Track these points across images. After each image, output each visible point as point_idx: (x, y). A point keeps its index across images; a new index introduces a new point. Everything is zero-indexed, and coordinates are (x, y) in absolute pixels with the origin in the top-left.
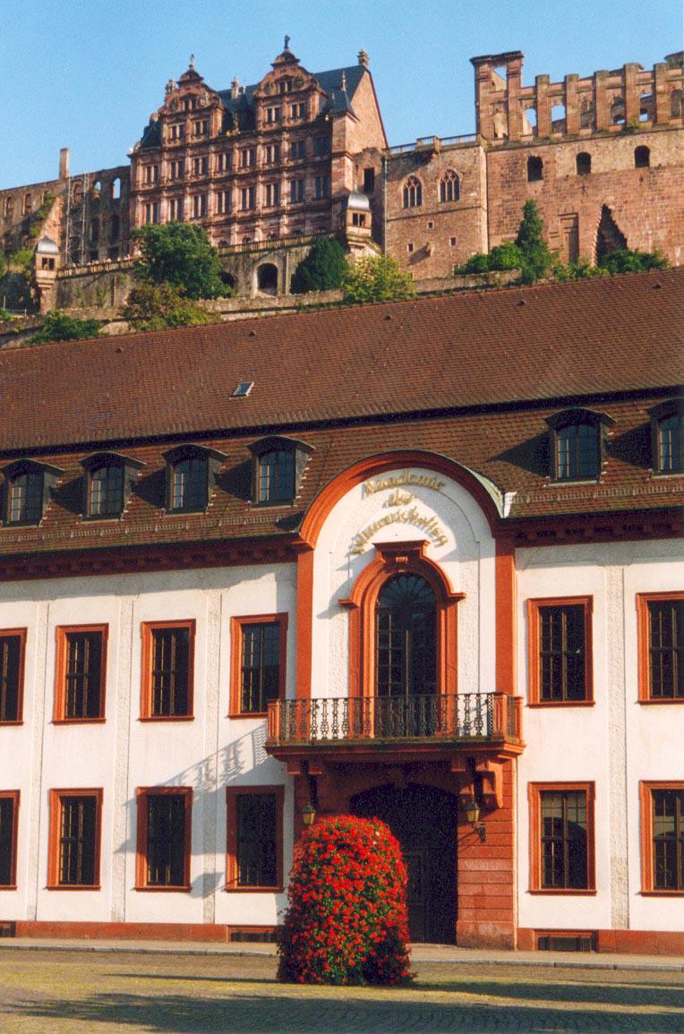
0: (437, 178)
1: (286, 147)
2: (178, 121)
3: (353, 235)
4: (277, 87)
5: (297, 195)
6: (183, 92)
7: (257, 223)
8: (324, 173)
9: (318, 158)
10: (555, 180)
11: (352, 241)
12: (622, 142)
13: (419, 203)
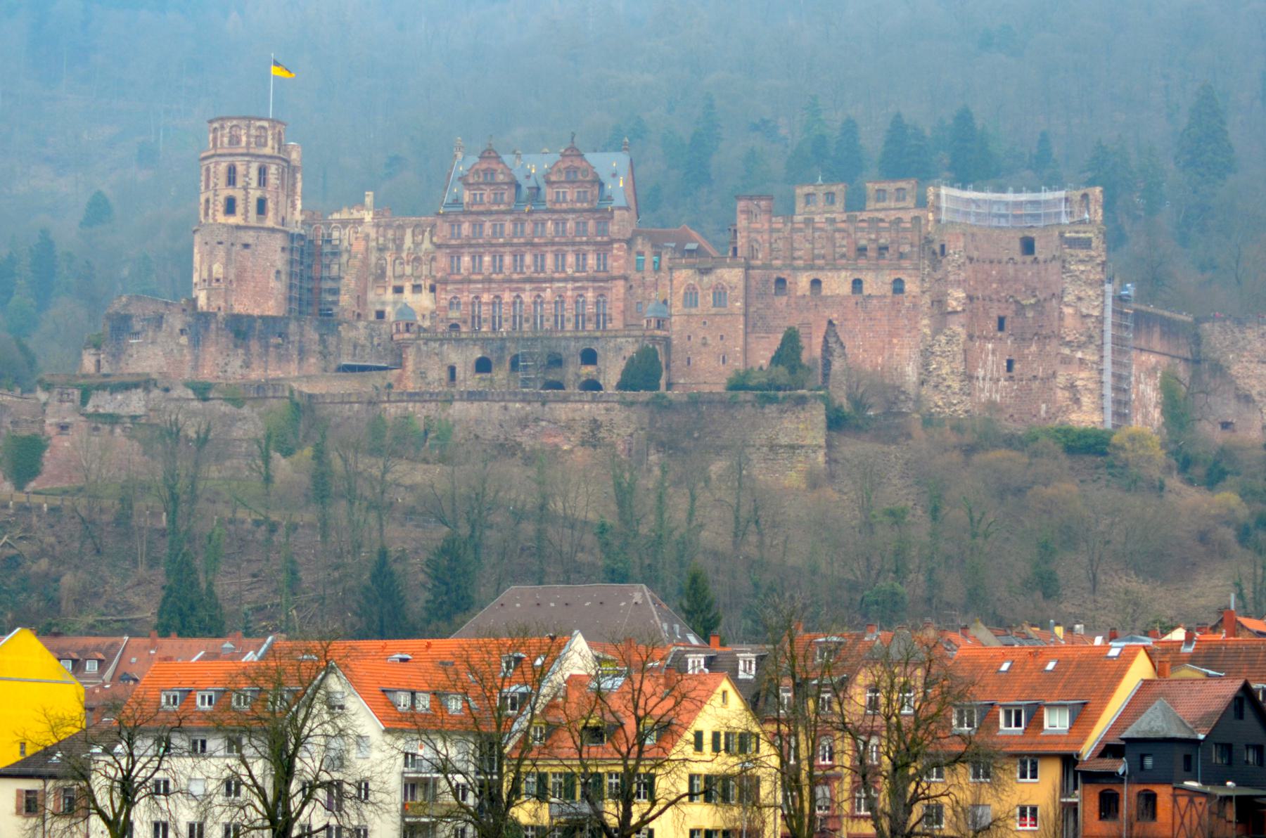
5: (581, 266)
6: (484, 166)
8: (603, 248)
9: (599, 239)
12: (843, 274)
13: (696, 305)
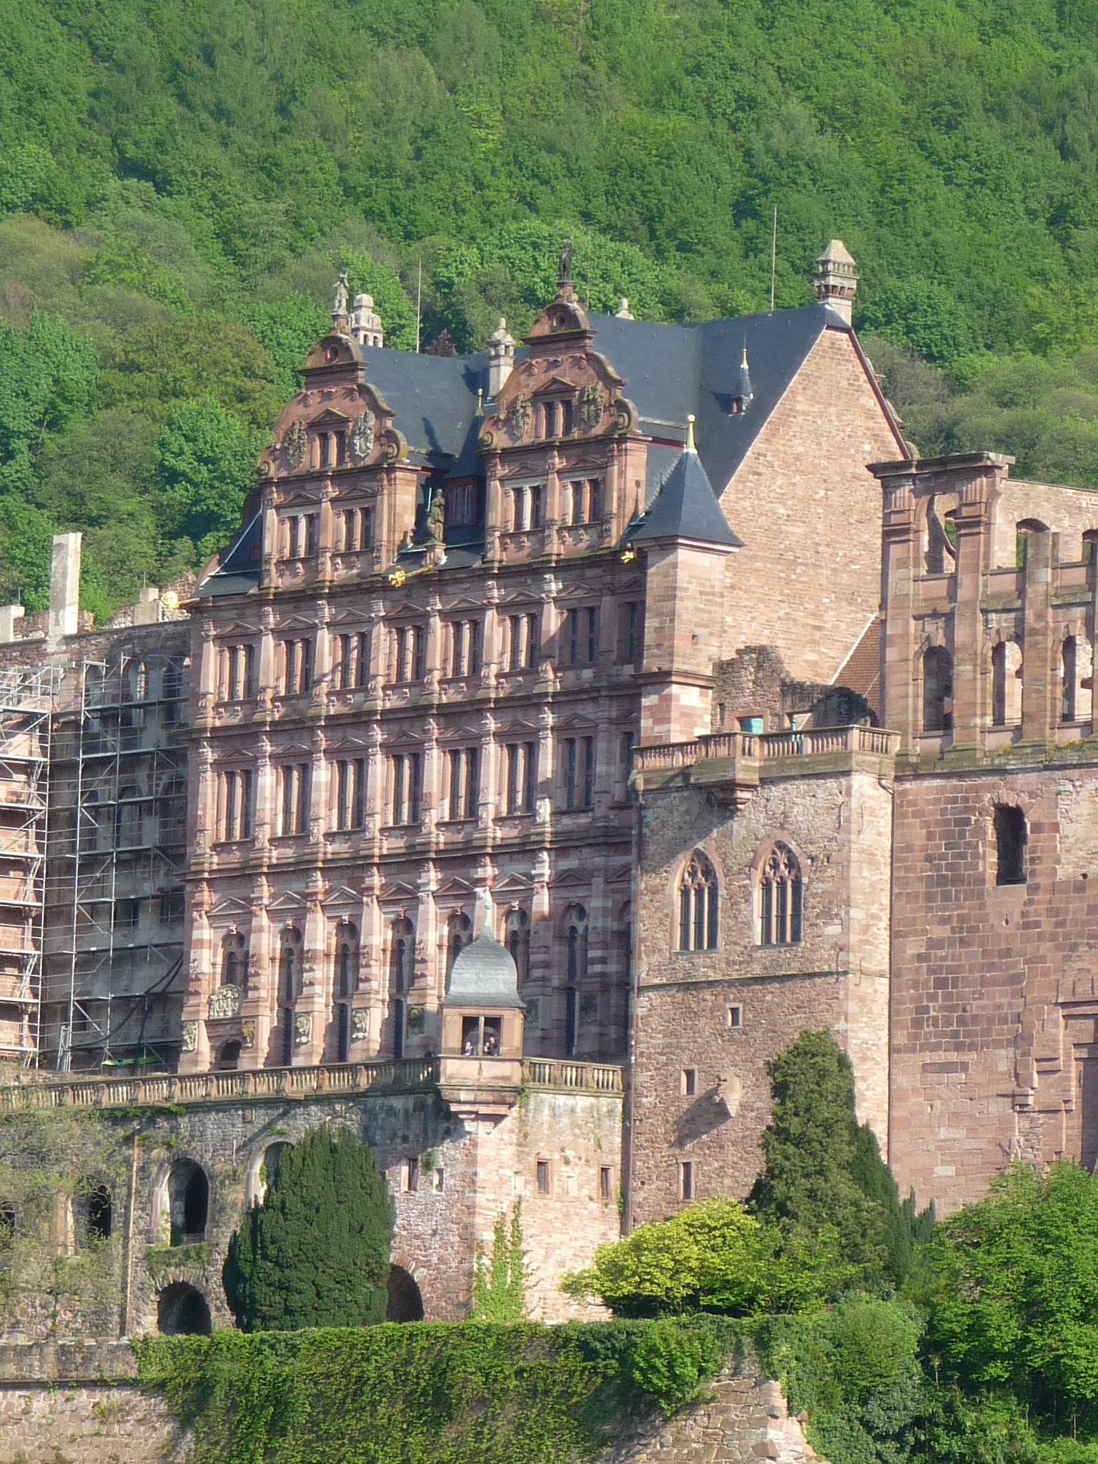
0: (752, 865)
1: (553, 620)
2: (302, 501)
3: (458, 1088)
4: (536, 411)
7: (480, 873)
10: (1054, 888)
11: (459, 1102)
